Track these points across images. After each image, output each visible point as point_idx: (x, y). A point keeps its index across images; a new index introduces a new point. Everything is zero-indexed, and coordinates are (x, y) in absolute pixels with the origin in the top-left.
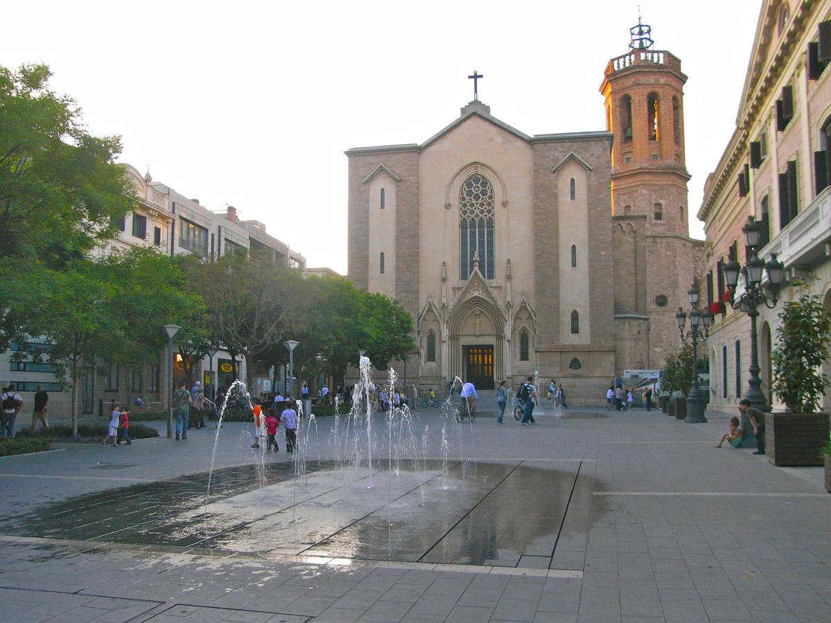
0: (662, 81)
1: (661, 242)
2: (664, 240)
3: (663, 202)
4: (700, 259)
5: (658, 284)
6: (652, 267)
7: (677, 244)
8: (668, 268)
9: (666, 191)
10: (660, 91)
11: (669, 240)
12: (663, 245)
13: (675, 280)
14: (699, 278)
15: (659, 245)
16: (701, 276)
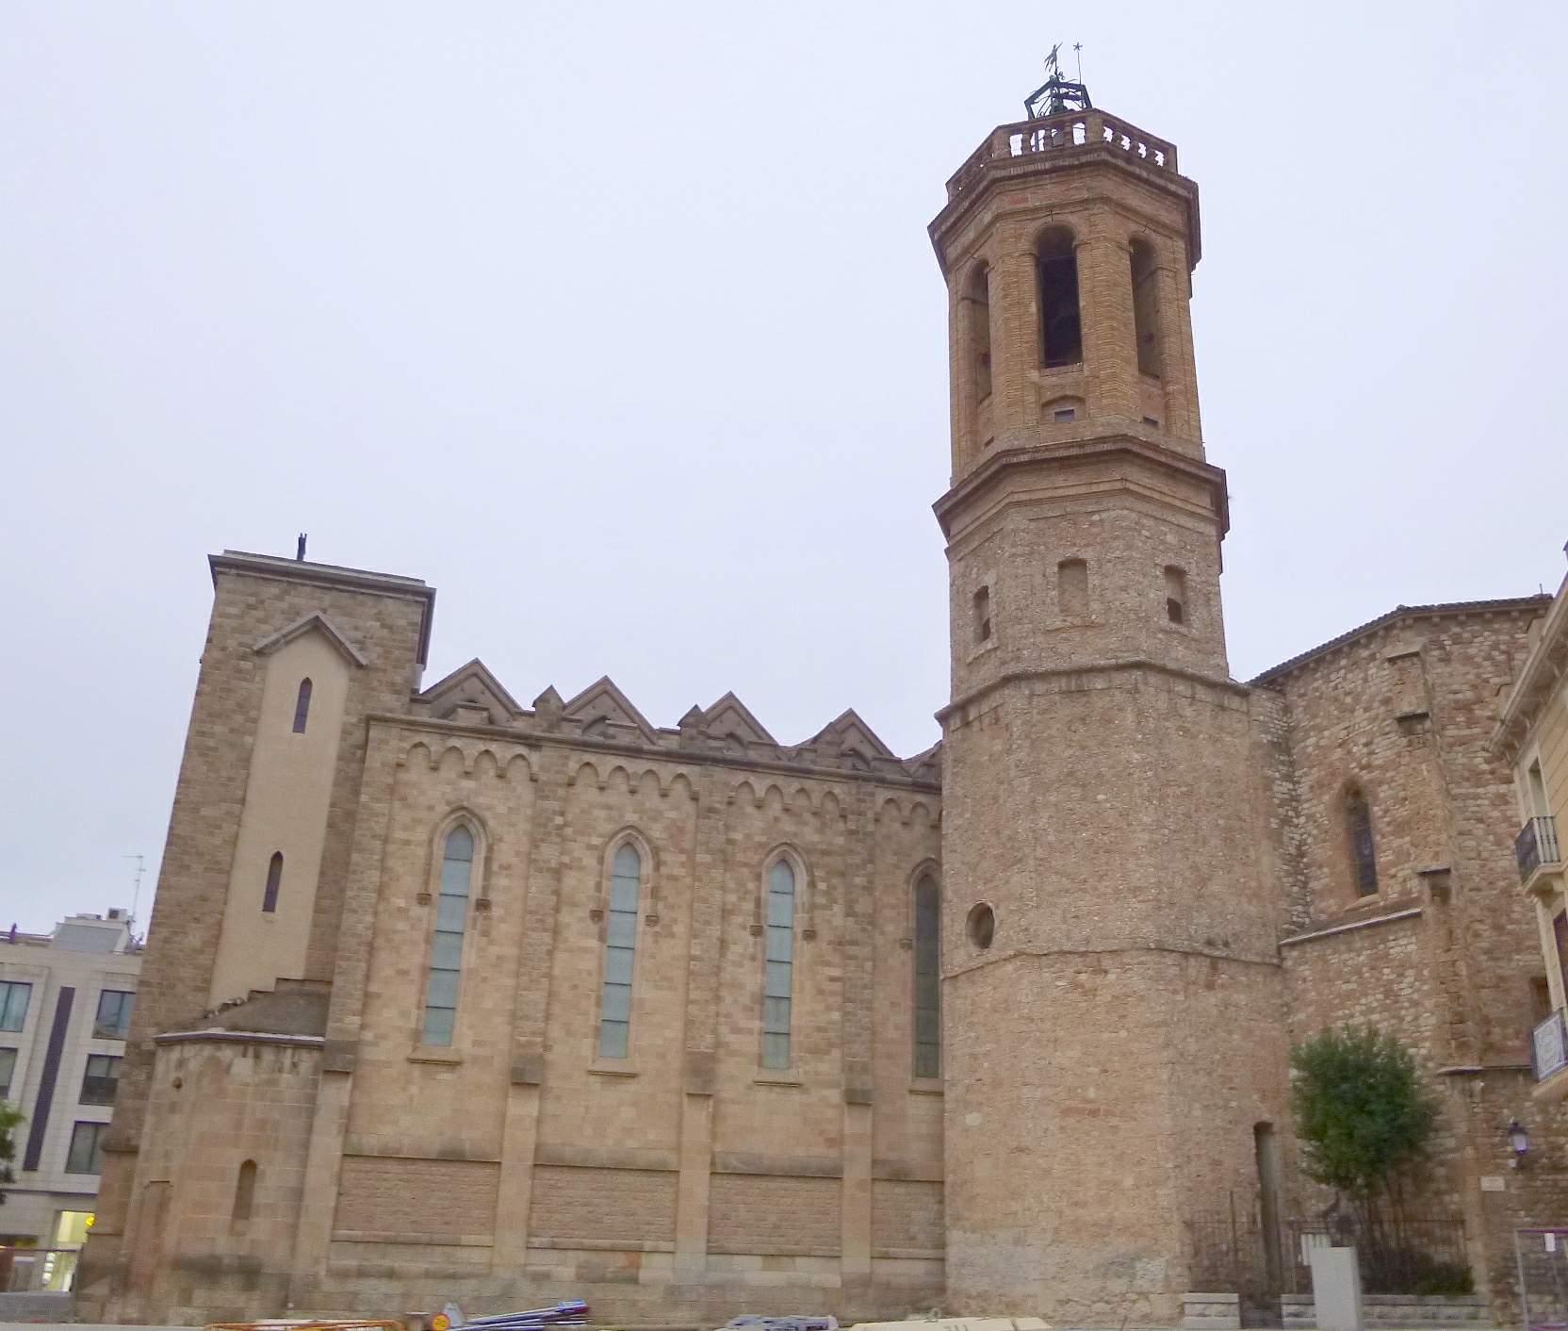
0: (987, 217)
1: (980, 717)
2: (985, 707)
3: (989, 579)
4: (1357, 700)
5: (974, 868)
6: (961, 815)
7: (1014, 699)
8: (995, 798)
9: (997, 539)
10: (986, 252)
11: (995, 699)
12: (986, 721)
13: (1010, 838)
14: (1366, 776)
15: (976, 726)
16: (1368, 767)
